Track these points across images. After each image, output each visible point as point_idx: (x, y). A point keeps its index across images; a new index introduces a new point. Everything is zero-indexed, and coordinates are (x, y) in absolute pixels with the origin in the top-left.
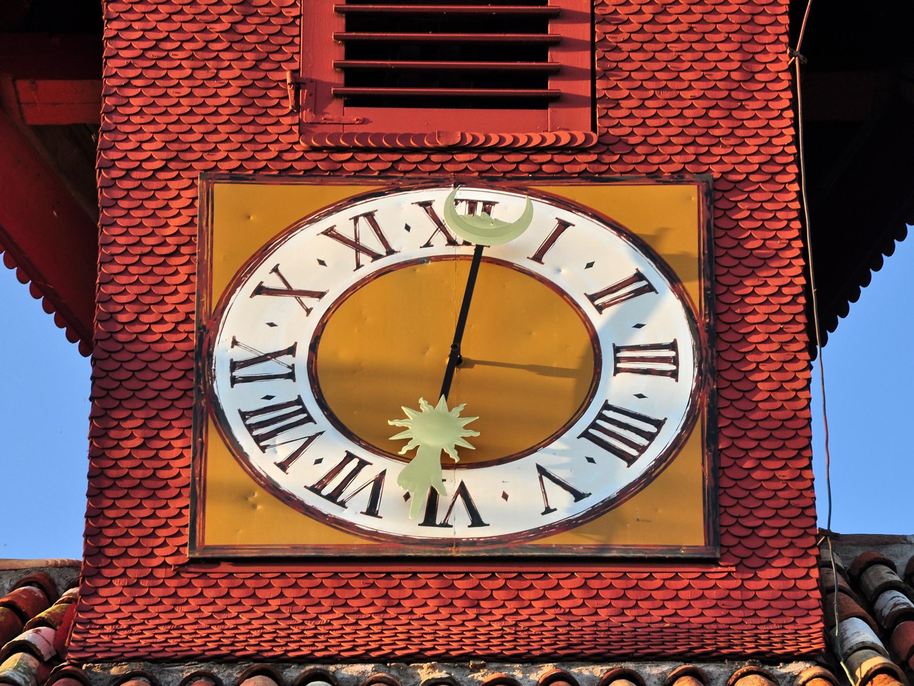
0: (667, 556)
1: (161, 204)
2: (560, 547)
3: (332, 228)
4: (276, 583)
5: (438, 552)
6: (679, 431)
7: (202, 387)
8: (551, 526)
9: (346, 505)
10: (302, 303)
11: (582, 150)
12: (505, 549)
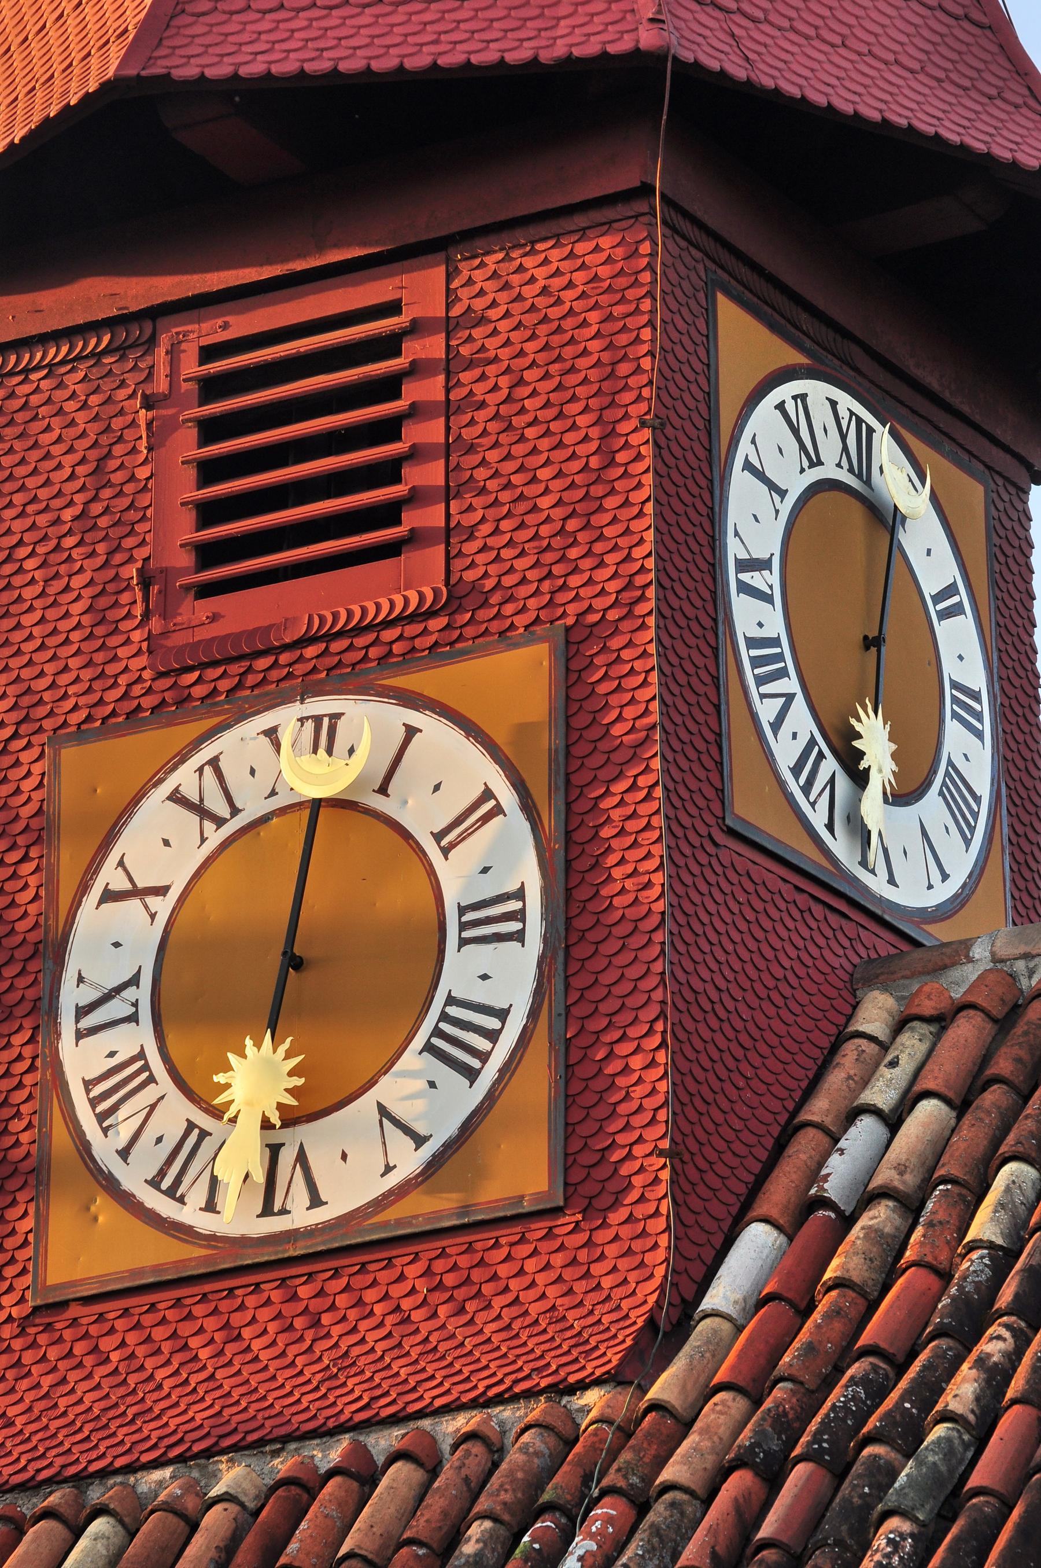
0: (509, 1213)
2: (399, 1223)
3: (177, 790)
8: (390, 1192)
10: (146, 907)
11: (431, 614)
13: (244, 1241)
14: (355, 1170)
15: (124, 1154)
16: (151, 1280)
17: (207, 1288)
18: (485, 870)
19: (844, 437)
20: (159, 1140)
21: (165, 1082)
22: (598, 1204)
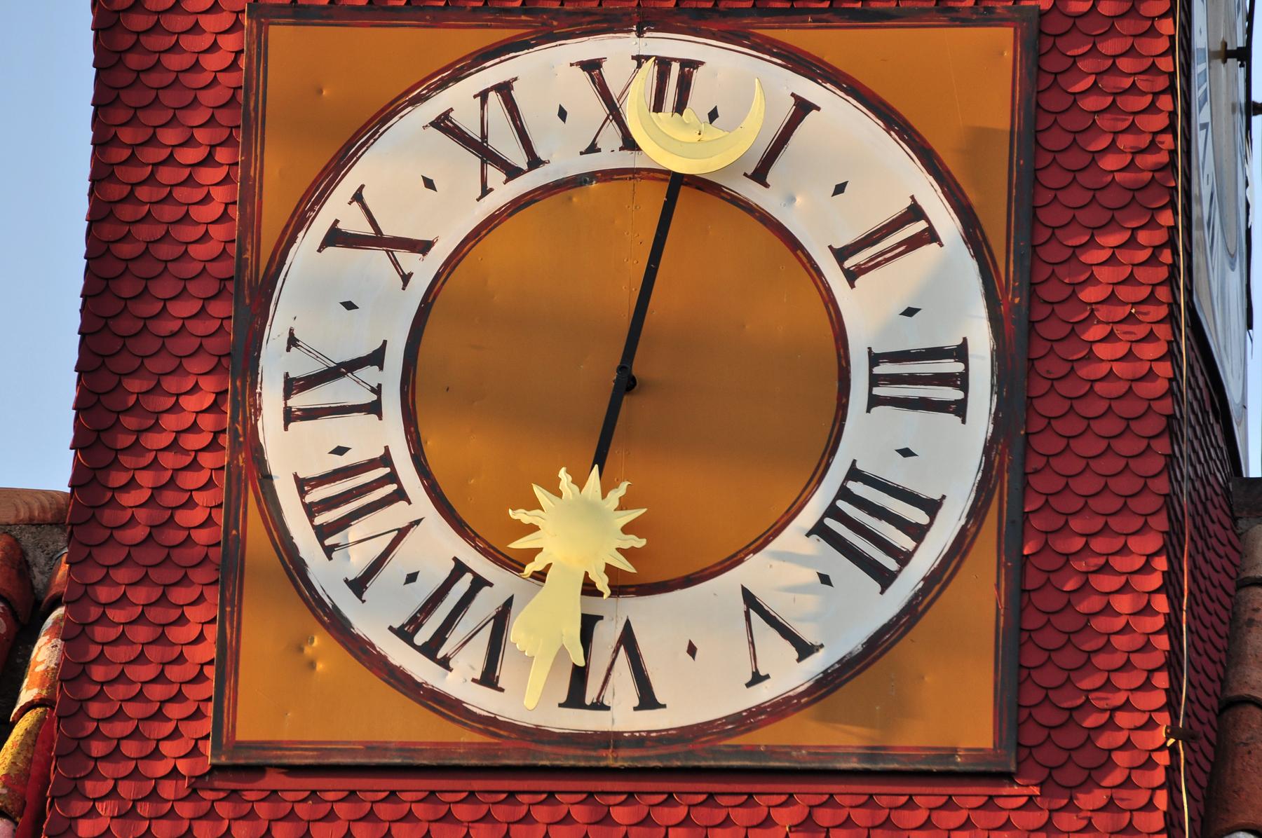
0: (935, 768)
1: (187, 61)
2: (772, 751)
3: (446, 115)
4: (342, 810)
5: (587, 758)
6: (963, 522)
7: (239, 428)
8: (759, 709)
9: (451, 664)
10: (396, 264)
12: (689, 754)
13: (538, 735)
14: (705, 669)
15: (358, 586)
16: (398, 761)
17: (477, 785)
18: (910, 312)
20: (412, 578)
22: (1063, 777)
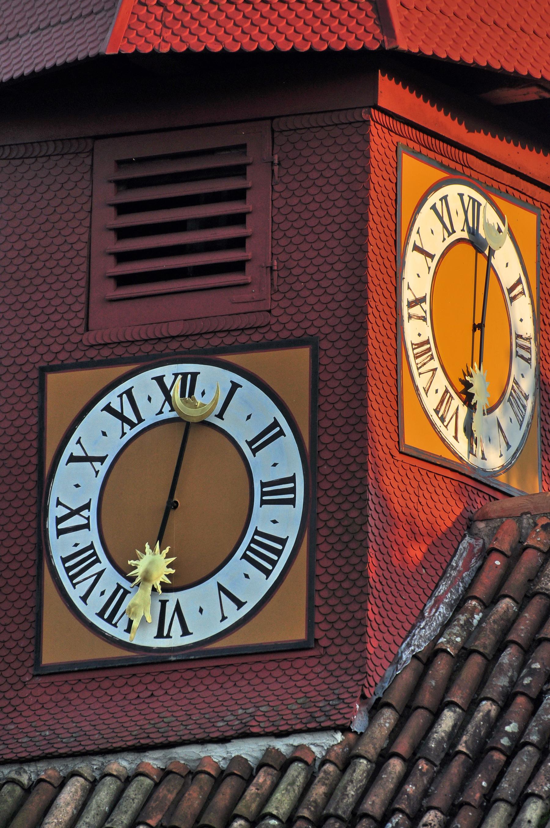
15: (84, 598)
19: (466, 212)
21: (105, 563)
